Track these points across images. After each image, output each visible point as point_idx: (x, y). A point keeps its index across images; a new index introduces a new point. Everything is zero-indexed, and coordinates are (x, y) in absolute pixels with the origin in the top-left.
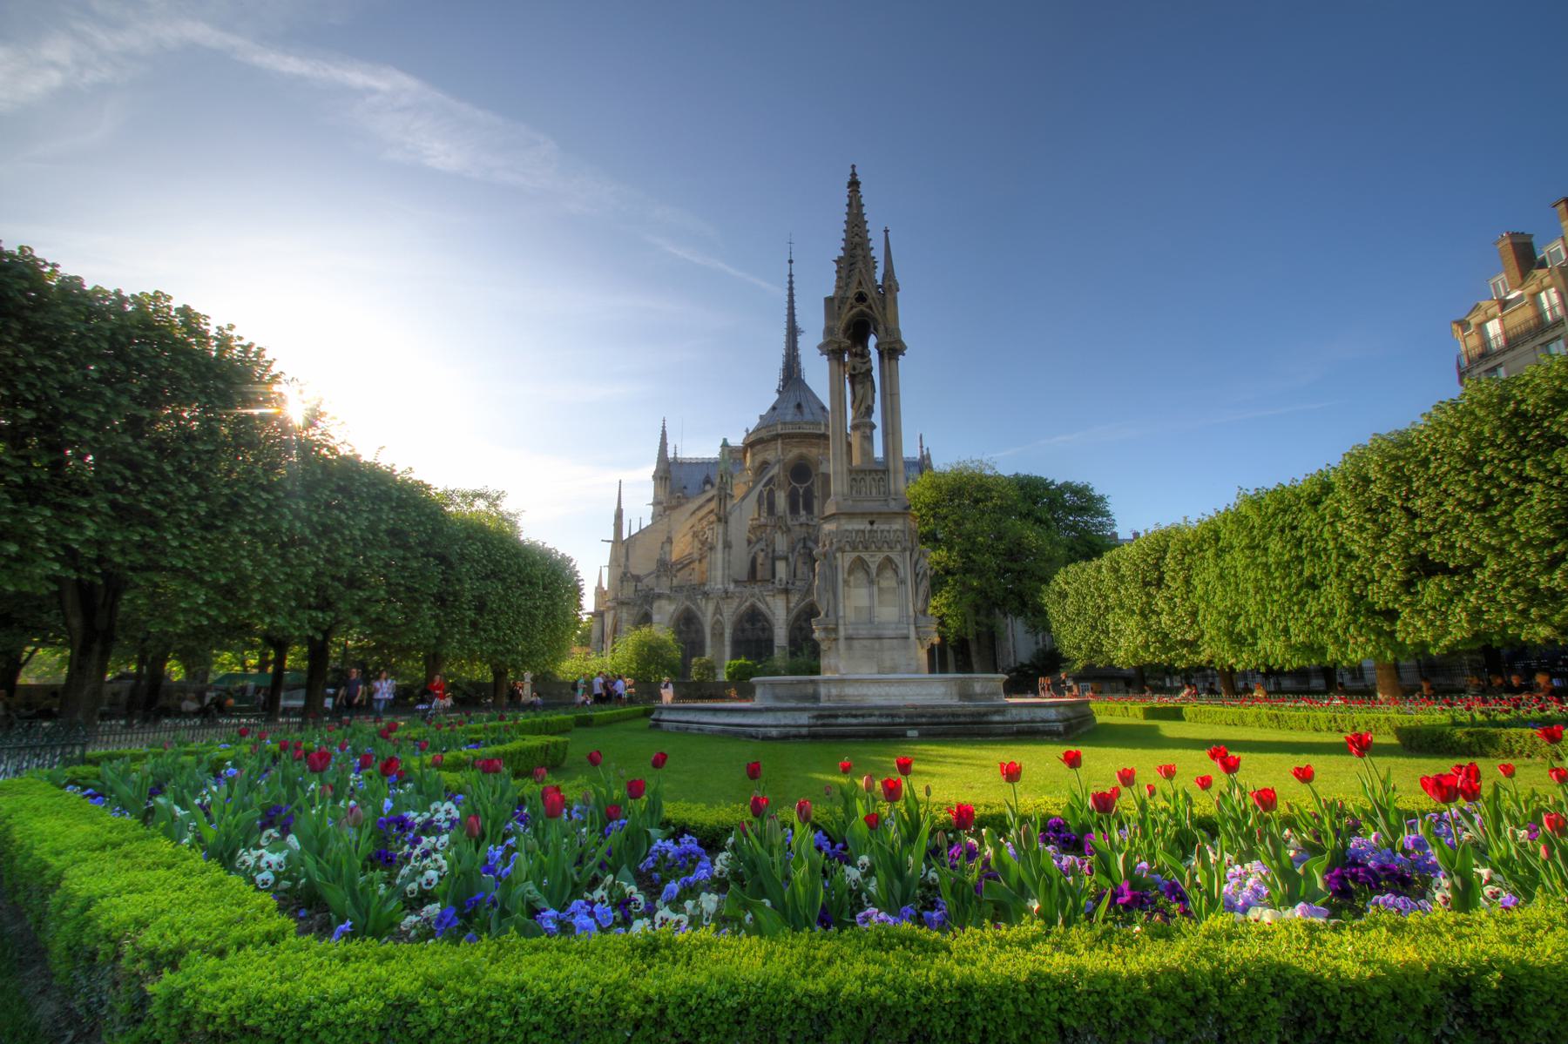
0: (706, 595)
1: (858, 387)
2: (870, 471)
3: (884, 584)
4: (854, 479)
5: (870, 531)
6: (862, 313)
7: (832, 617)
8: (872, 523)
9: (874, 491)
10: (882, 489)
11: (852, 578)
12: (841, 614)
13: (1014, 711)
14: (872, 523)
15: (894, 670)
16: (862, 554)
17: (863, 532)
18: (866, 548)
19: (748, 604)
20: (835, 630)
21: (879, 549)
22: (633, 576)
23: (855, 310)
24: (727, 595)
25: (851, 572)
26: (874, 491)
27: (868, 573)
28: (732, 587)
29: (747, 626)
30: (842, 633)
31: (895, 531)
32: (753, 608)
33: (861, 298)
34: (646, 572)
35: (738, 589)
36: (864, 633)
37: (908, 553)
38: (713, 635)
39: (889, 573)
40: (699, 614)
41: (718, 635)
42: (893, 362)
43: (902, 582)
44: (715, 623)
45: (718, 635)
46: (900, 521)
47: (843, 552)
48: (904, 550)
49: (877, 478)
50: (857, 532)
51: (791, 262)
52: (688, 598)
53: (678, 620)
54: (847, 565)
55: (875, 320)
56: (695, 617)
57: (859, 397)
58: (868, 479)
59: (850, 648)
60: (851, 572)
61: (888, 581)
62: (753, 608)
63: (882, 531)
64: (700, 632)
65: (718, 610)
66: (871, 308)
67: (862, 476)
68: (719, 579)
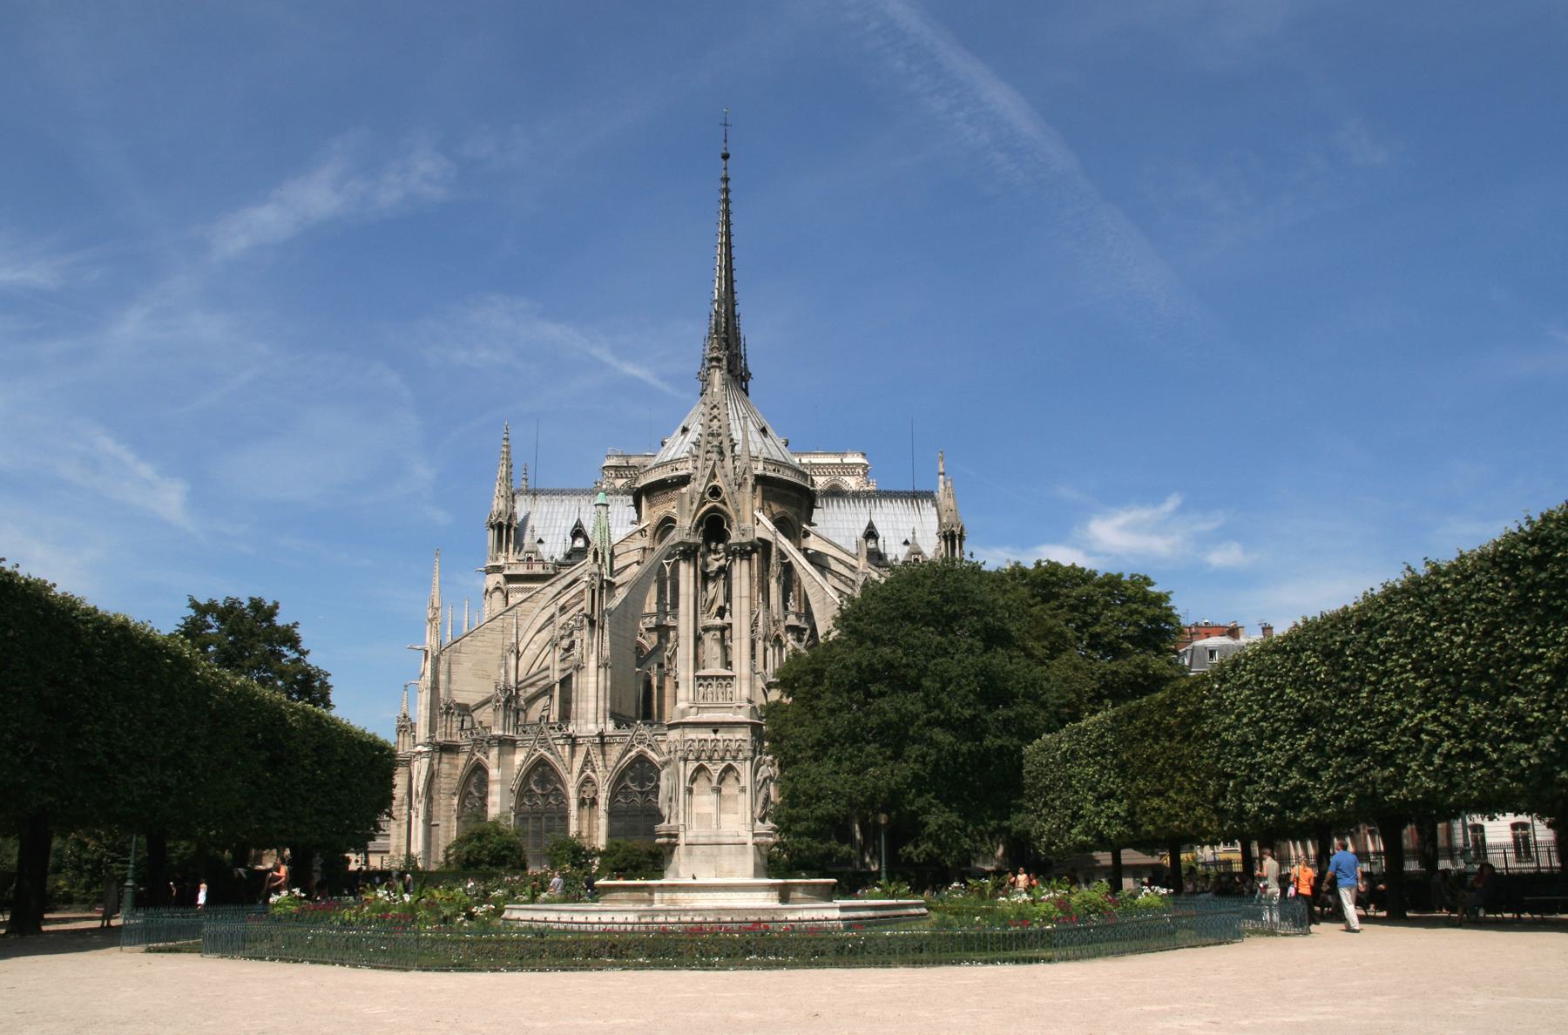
0: (573, 742)
1: (711, 586)
2: (718, 677)
3: (725, 791)
4: (701, 685)
5: (712, 741)
6: (714, 509)
7: (673, 822)
8: (715, 732)
9: (720, 695)
10: (729, 696)
11: (694, 786)
12: (681, 822)
13: (805, 913)
14: (715, 732)
15: (731, 873)
16: (704, 763)
17: (706, 740)
18: (710, 759)
19: (633, 753)
20: (676, 836)
21: (723, 759)
22: (459, 705)
23: (708, 506)
24: (603, 741)
25: (693, 780)
26: (720, 695)
27: (710, 780)
28: (610, 727)
29: (635, 787)
30: (682, 840)
31: (737, 741)
32: (641, 759)
33: (715, 492)
34: (479, 698)
35: (618, 732)
36: (702, 840)
37: (748, 763)
38: (582, 803)
39: (730, 780)
40: (560, 767)
41: (588, 803)
42: (745, 564)
43: (743, 790)
44: (582, 785)
45: (588, 803)
46: (744, 730)
47: (686, 760)
48: (745, 759)
49: (724, 683)
50: (700, 741)
51: (726, 157)
52: (544, 742)
53: (526, 778)
54: (689, 773)
55: (727, 516)
56: (553, 770)
57: (711, 596)
58: (714, 683)
59: (689, 853)
60: (693, 780)
61: (730, 788)
62: (641, 759)
63: (725, 740)
64: (562, 797)
65: (587, 762)
66: (725, 504)
67: (710, 681)
68: (591, 716)
